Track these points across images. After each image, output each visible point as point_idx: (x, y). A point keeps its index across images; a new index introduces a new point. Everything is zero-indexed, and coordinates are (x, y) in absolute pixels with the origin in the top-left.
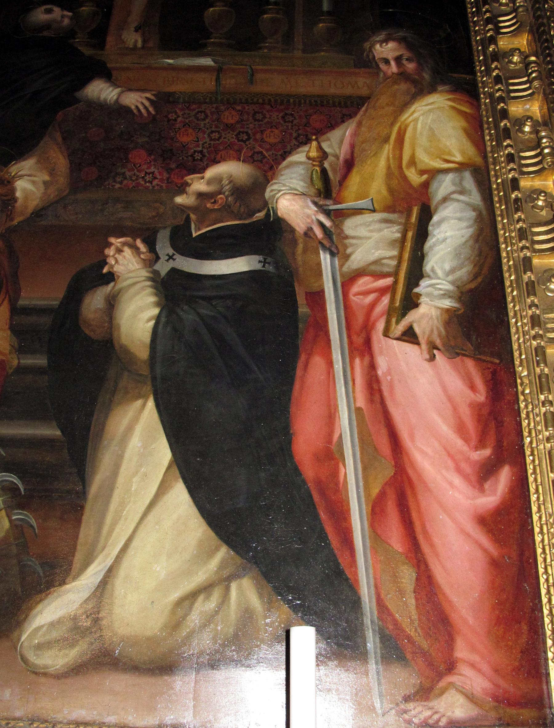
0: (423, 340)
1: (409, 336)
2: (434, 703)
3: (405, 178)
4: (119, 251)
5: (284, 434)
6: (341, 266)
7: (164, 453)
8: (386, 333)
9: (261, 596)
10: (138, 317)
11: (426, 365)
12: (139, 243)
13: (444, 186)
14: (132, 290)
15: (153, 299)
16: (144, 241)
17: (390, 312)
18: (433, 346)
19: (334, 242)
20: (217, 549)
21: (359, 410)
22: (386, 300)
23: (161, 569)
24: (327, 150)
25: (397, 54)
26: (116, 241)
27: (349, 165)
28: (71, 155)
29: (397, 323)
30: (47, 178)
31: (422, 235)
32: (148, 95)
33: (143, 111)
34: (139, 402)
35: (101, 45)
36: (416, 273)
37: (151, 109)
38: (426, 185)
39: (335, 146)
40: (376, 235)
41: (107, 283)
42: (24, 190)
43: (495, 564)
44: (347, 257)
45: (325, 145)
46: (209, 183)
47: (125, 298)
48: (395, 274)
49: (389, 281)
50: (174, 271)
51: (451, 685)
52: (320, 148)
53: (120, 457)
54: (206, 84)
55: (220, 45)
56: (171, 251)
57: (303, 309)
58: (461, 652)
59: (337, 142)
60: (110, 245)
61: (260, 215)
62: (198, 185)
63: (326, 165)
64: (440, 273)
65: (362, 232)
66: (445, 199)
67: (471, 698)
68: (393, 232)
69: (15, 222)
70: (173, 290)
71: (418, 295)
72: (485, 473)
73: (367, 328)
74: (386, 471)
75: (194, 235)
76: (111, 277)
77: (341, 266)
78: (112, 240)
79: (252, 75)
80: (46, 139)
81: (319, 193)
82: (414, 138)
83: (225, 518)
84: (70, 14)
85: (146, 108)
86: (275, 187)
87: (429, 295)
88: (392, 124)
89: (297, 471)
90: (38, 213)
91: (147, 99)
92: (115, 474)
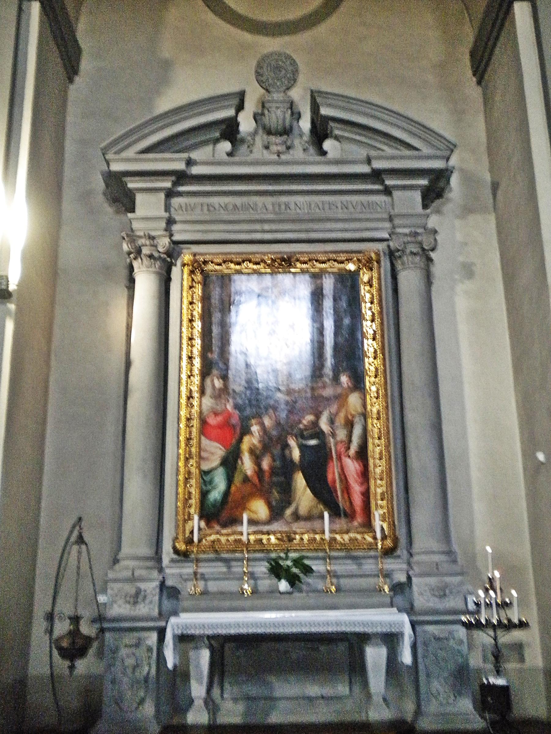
7: (304, 482)
10: (296, 454)
19: (334, 435)
34: (297, 472)
36: (350, 441)
70: (302, 447)
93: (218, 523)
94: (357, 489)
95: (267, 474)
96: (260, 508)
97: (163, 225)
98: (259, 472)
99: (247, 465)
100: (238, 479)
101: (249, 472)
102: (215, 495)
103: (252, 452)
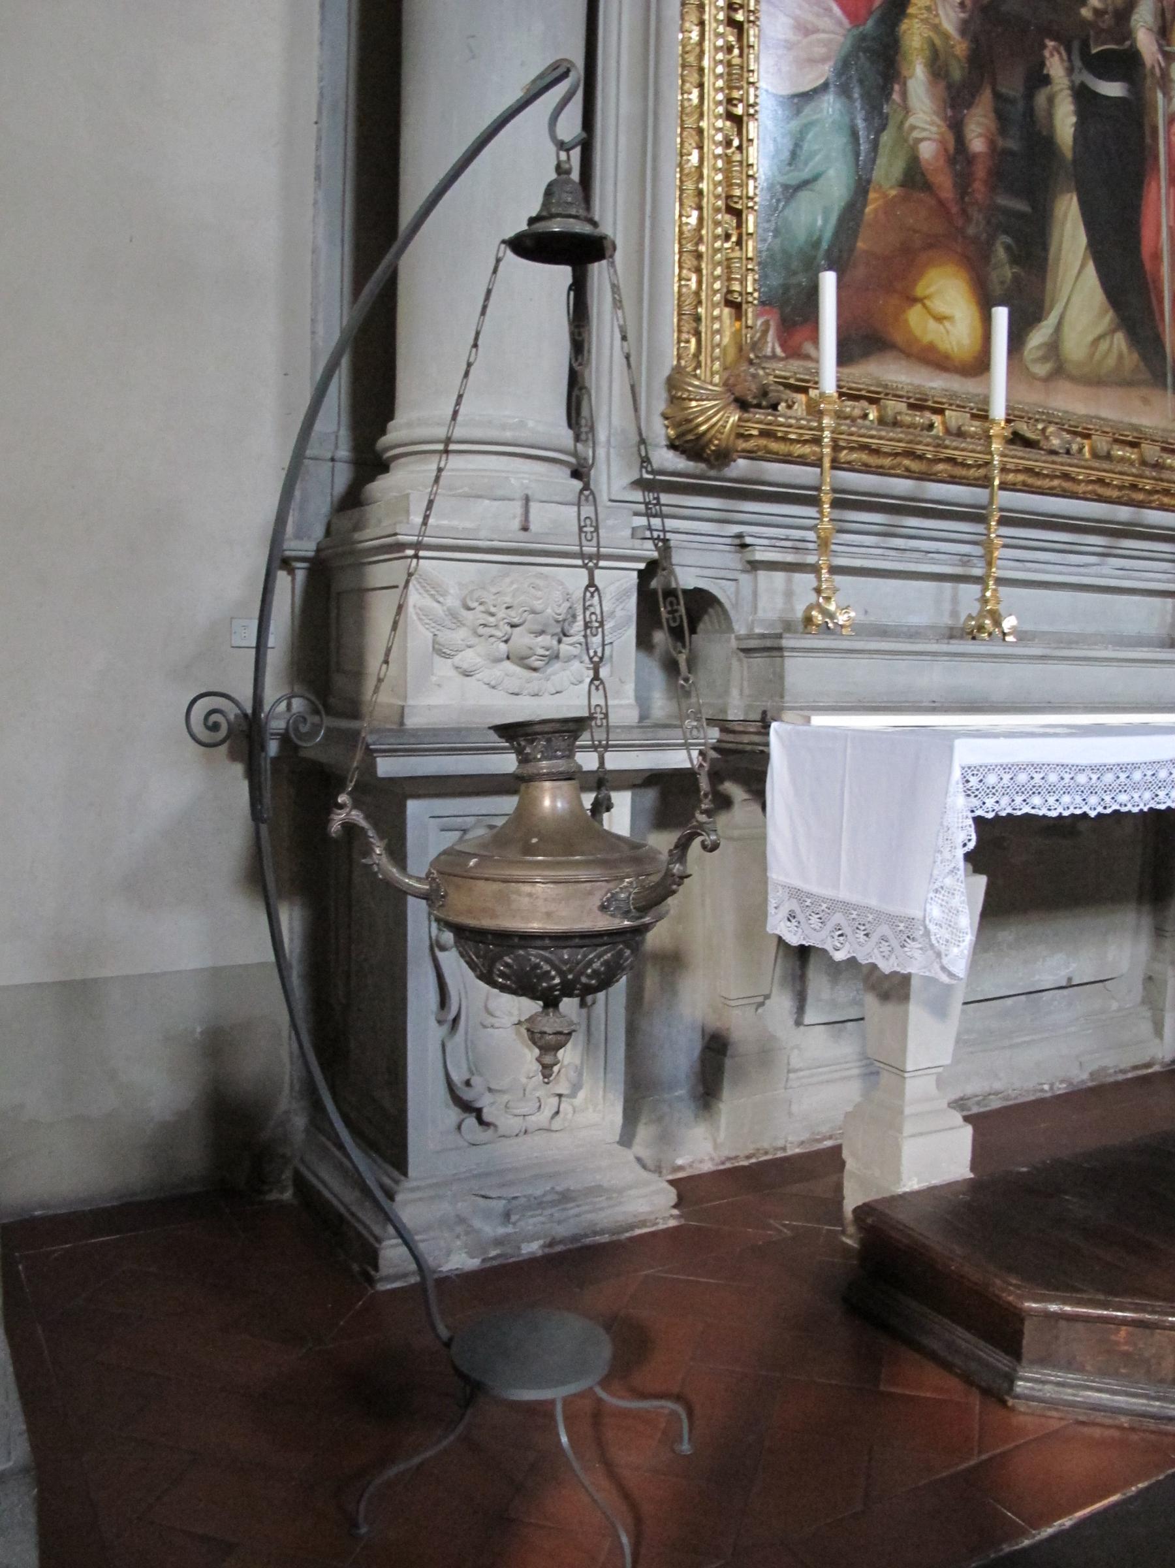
4: (1052, 55)
7: (1083, 240)
10: (1065, 121)
12: (1062, 49)
20: (1107, 312)
26: (1051, 44)
34: (1069, 195)
47: (1057, 100)
53: (1062, 236)
57: (1148, 140)
75: (1094, 51)
101: (927, 151)
103: (937, 68)
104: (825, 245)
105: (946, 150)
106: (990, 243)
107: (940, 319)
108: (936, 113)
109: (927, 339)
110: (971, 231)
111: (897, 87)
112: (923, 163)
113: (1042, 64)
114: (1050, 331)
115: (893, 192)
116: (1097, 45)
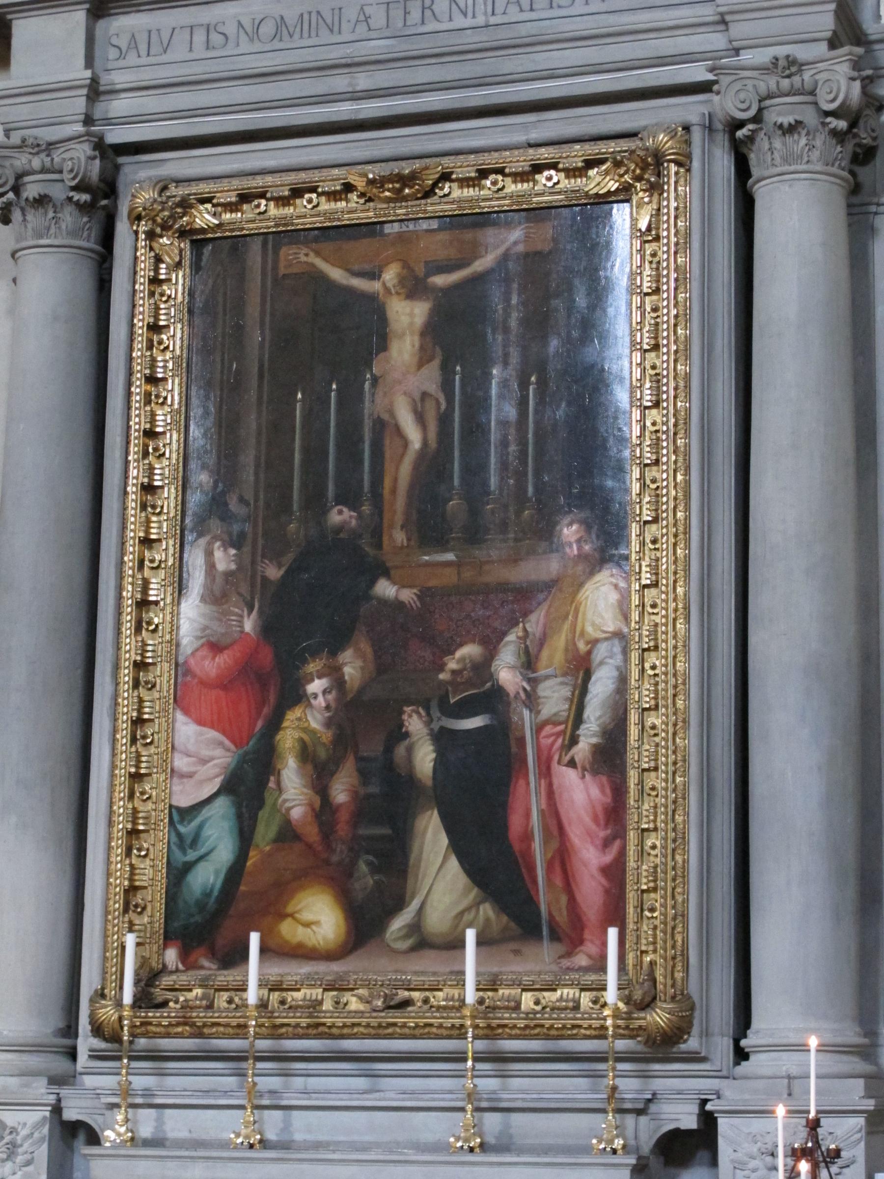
0: (579, 766)
1: (572, 764)
2: (572, 959)
3: (577, 650)
4: (410, 716)
5: (505, 827)
6: (536, 718)
7: (444, 840)
8: (559, 763)
9: (494, 912)
10: (424, 759)
11: (580, 781)
13: (601, 651)
14: (420, 742)
15: (431, 748)
16: (423, 708)
17: (563, 746)
18: (584, 769)
19: (531, 700)
21: (543, 810)
22: (560, 741)
23: (447, 900)
24: (529, 629)
25: (578, 536)
26: (408, 709)
27: (542, 643)
28: (373, 646)
29: (566, 755)
30: (362, 664)
31: (584, 691)
32: (415, 591)
33: (413, 605)
34: (429, 812)
35: (379, 546)
36: (579, 719)
37: (418, 604)
38: (589, 653)
39: (534, 626)
40: (556, 695)
41: (405, 739)
42: (350, 674)
43: (607, 892)
44: (538, 712)
45: (527, 626)
46: (458, 661)
48: (566, 722)
49: (562, 727)
50: (442, 728)
51: (580, 951)
52: (525, 630)
53: (423, 843)
54: (449, 577)
55: (459, 538)
56: (439, 715)
57: (514, 749)
58: (587, 935)
59: (535, 623)
60: (404, 712)
61: (489, 685)
62: (452, 665)
63: (528, 643)
64: (592, 719)
65: (547, 693)
66: (602, 663)
67: (590, 956)
68: (566, 692)
69: (348, 699)
70: (443, 739)
71: (579, 736)
72: (606, 844)
73: (549, 759)
74: (555, 845)
75: (452, 701)
76: (407, 735)
77: (536, 718)
78: (405, 709)
79: (481, 567)
80: (356, 632)
81: (523, 666)
82: (584, 614)
83: (477, 872)
84: (355, 514)
85: (415, 602)
86: (497, 663)
87: (585, 735)
88: (572, 602)
89: (510, 846)
90: (361, 691)
91: (415, 594)
92: (421, 853)
93: (212, 954)
94: (590, 857)
95: (344, 816)
96: (320, 917)
97: (79, 104)
98: (324, 810)
99: (292, 788)
100: (265, 833)
101: (297, 813)
102: (207, 877)
103: (305, 754)
104: (216, 893)
105: (313, 810)
106: (353, 863)
107: (307, 925)
108: (305, 787)
109: (295, 940)
110: (335, 858)
111: (272, 778)
112: (294, 823)
113: (401, 725)
114: (413, 915)
115: (268, 848)
116: (454, 697)
